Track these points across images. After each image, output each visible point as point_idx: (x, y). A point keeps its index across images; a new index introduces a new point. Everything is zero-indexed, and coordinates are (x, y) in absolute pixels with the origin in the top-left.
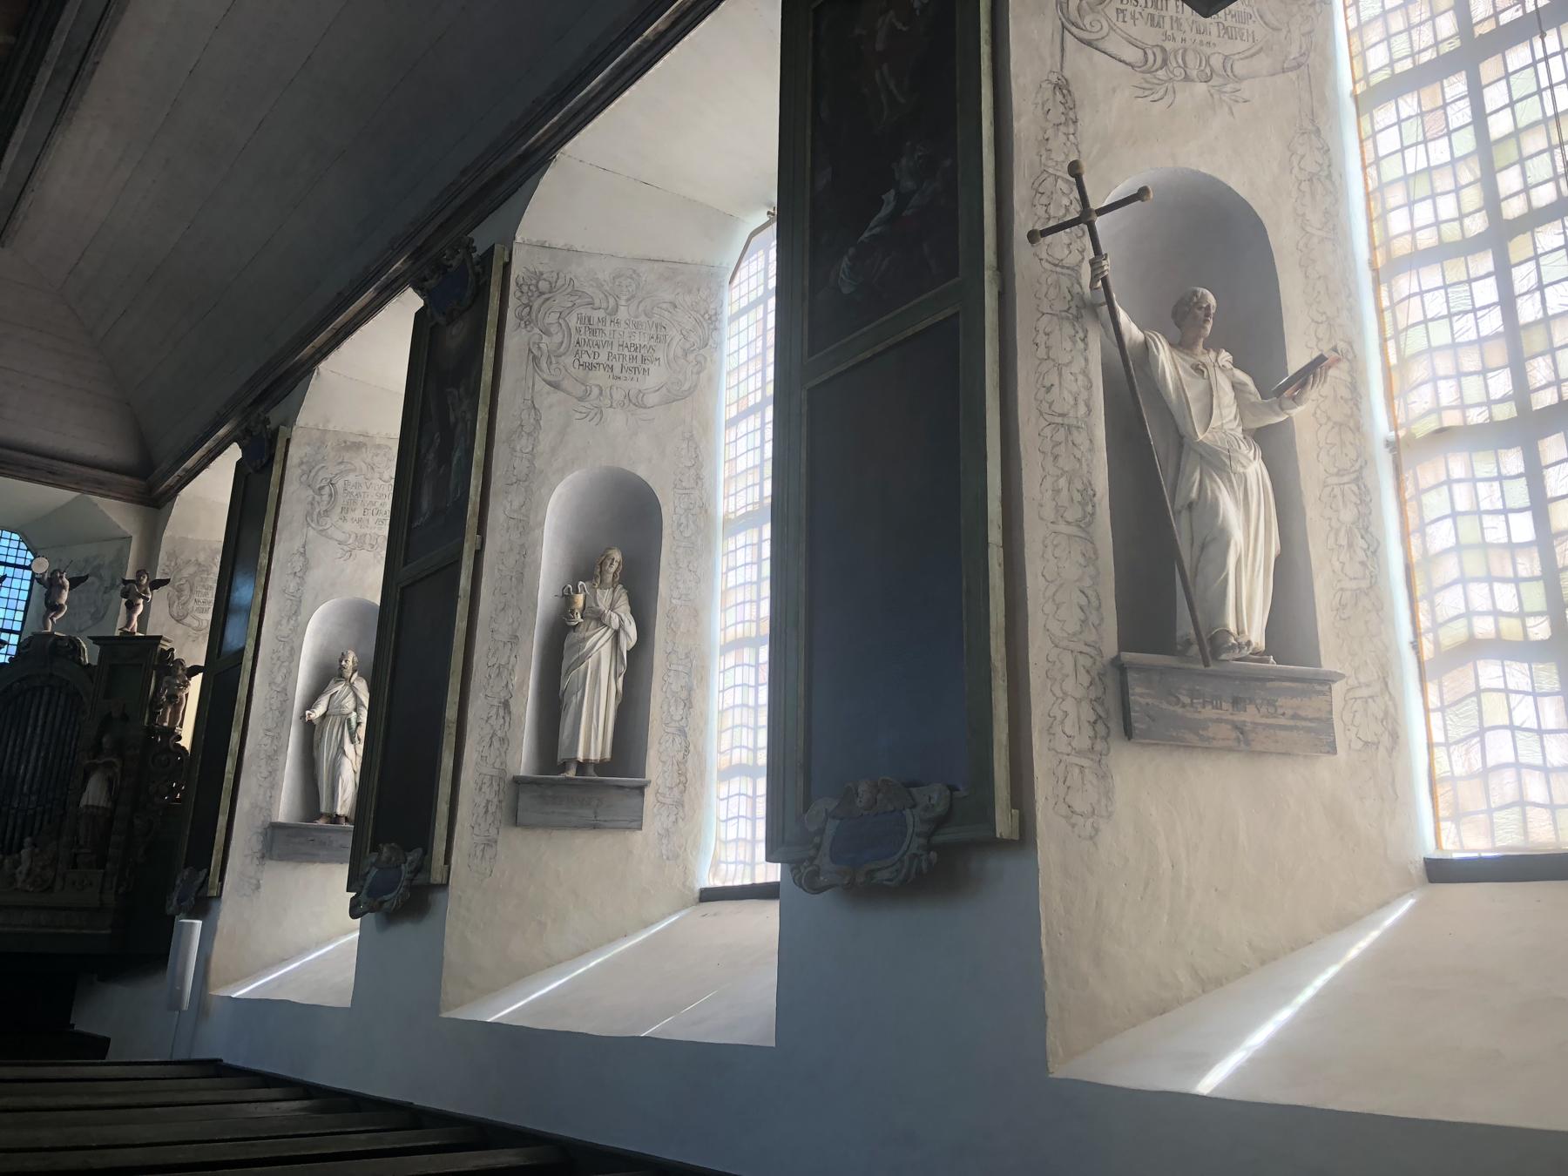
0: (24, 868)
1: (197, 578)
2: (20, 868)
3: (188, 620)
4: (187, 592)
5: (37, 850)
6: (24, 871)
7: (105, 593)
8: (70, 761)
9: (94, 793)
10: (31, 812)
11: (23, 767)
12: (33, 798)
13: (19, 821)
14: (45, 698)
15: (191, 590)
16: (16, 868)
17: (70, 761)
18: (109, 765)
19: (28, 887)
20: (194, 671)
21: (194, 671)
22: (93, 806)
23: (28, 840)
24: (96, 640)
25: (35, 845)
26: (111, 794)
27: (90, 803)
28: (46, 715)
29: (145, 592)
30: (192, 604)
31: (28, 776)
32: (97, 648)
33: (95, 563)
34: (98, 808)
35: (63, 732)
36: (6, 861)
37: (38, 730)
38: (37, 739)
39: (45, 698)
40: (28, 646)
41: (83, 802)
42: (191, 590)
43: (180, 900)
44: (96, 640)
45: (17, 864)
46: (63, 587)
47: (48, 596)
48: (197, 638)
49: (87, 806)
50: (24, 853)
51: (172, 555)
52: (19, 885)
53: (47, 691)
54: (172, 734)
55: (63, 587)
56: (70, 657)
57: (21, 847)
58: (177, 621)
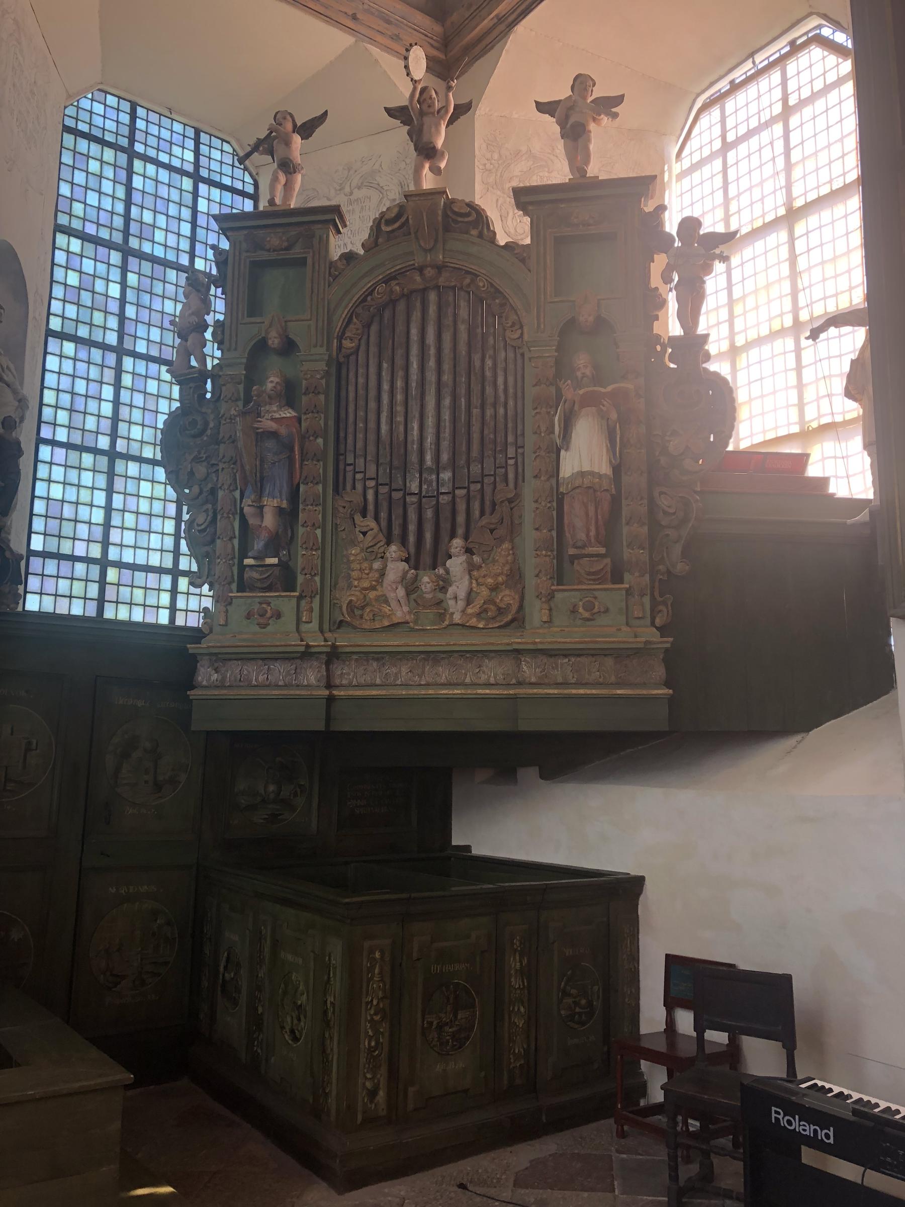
0: (460, 587)
2: (451, 590)
5: (477, 559)
6: (462, 594)
8: (501, 411)
10: (444, 499)
11: (416, 426)
12: (446, 475)
13: (429, 514)
14: (432, 310)
16: (444, 589)
17: (501, 411)
19: (473, 622)
22: (592, 473)
25: (469, 551)
26: (614, 454)
27: (586, 468)
31: (429, 439)
34: (600, 476)
35: (477, 363)
36: (426, 579)
37: (432, 363)
38: (431, 377)
39: (432, 310)
45: (444, 585)
49: (582, 474)
50: (456, 565)
52: (457, 618)
53: (432, 296)
56: (474, 232)
57: (439, 557)
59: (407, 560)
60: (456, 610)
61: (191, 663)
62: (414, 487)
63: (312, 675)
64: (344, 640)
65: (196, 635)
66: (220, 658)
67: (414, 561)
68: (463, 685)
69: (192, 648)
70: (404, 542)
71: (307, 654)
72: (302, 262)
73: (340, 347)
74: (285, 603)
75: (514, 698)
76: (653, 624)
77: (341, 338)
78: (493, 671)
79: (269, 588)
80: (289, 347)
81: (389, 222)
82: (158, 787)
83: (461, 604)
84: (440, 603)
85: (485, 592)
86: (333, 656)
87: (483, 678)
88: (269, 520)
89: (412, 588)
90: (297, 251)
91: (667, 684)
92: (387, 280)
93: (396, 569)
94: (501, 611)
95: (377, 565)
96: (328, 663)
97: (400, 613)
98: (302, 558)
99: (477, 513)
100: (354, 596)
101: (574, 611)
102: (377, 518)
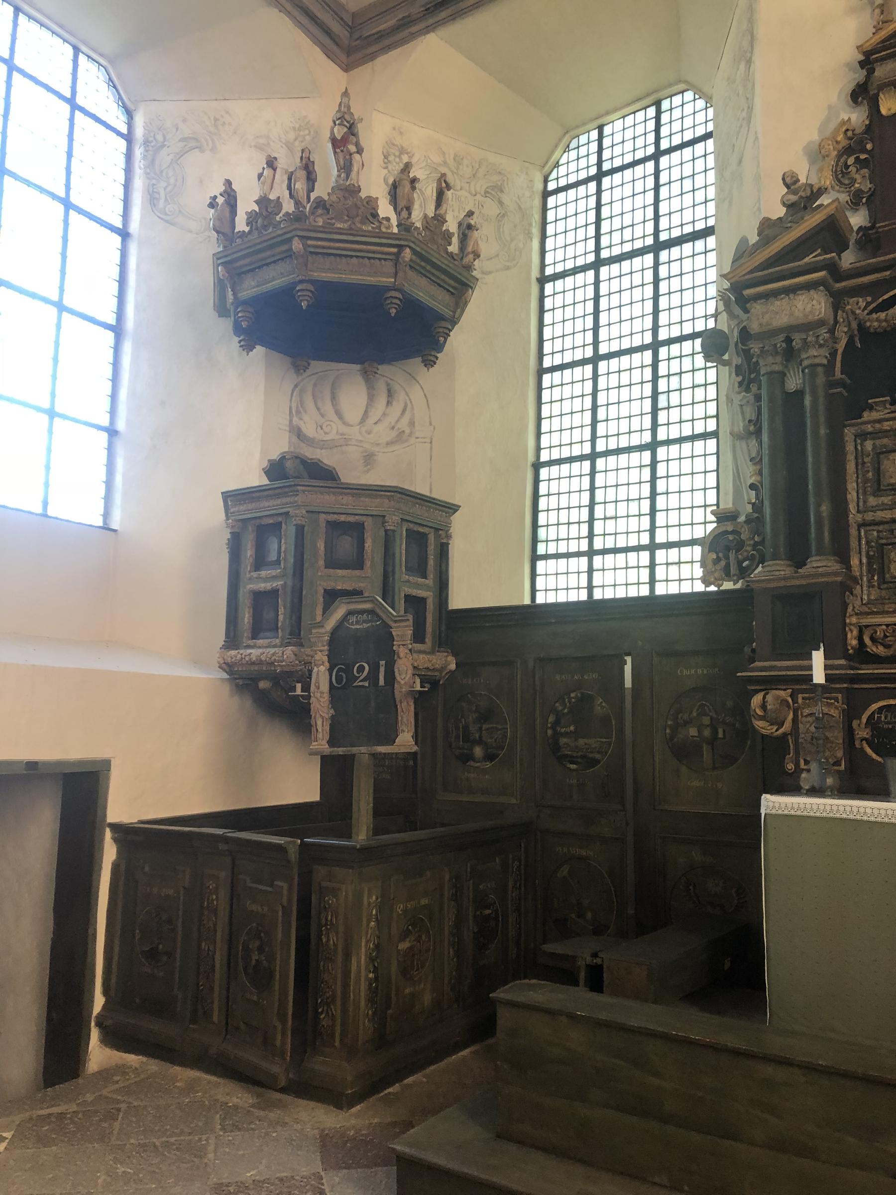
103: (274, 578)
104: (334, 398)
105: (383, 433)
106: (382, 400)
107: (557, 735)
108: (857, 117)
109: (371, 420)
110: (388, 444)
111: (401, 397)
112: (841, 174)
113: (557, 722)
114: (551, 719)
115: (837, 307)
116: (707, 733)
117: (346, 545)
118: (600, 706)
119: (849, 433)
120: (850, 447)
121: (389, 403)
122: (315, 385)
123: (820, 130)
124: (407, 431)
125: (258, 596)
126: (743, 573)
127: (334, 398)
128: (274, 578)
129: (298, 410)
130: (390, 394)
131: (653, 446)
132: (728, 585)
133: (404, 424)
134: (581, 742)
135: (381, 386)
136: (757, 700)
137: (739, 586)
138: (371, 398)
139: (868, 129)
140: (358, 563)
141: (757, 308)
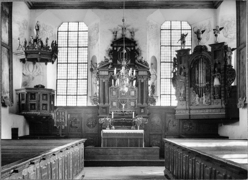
1: (229, 25)
3: (228, 36)
4: (227, 29)
5: (206, 96)
7: (208, 33)
9: (216, 82)
15: (228, 29)
16: (203, 100)
18: (218, 75)
19: (206, 104)
20: (233, 49)
21: (233, 49)
23: (204, 94)
24: (210, 45)
25: (205, 95)
28: (202, 65)
29: (219, 31)
30: (228, 32)
32: (210, 47)
33: (204, 26)
36: (200, 99)
40: (196, 49)
41: (214, 85)
42: (228, 29)
43: (240, 105)
44: (210, 45)
45: (203, 99)
46: (200, 33)
47: (198, 36)
48: (231, 41)
49: (215, 85)
50: (204, 97)
51: (222, 20)
52: (204, 104)
53: (201, 59)
54: (230, 66)
55: (200, 33)
58: (226, 37)
59: (199, 96)
60: (204, 102)
61: (175, 111)
62: (199, 86)
63: (187, 112)
64: (191, 107)
65: (176, 107)
66: (178, 110)
67: (200, 96)
68: (204, 113)
69: (175, 109)
70: (199, 95)
71: (187, 109)
72: (185, 56)
73: (190, 67)
74: (185, 102)
75: (209, 114)
76: (225, 104)
77: (191, 66)
78: (207, 111)
79: (183, 101)
80: (184, 68)
81: (195, 50)
82: (174, 126)
83: (205, 102)
84: (202, 102)
85: (207, 100)
86: (190, 109)
87: (206, 112)
88: (182, 93)
89: (199, 100)
90: (185, 55)
91: (225, 112)
92: (195, 58)
93: (197, 98)
94: (209, 103)
95: (195, 97)
96: (189, 110)
97: (198, 103)
98: (187, 97)
99: (207, 89)
100: (193, 101)
101: (215, 103)
102: (195, 91)
103: (34, 102)
104: (28, 68)
105: (35, 74)
106: (35, 68)
107: (71, 124)
108: (111, 48)
109: (34, 72)
110: (36, 76)
111: (38, 68)
112: (109, 55)
113: (72, 122)
114: (70, 122)
115: (109, 73)
116: (92, 123)
117: (45, 97)
118: (78, 120)
119: (110, 88)
120: (110, 90)
121: (36, 69)
122: (25, 65)
123: (107, 48)
124: (39, 74)
125: (32, 104)
126: (97, 104)
127: (28, 68)
128: (34, 102)
129: (23, 70)
130: (37, 67)
131: (77, 79)
132: (95, 105)
133: (39, 72)
134: (75, 125)
135: (35, 65)
136: (99, 119)
137: (96, 105)
138: (34, 68)
139: (112, 50)
140: (47, 100)
141: (100, 72)
